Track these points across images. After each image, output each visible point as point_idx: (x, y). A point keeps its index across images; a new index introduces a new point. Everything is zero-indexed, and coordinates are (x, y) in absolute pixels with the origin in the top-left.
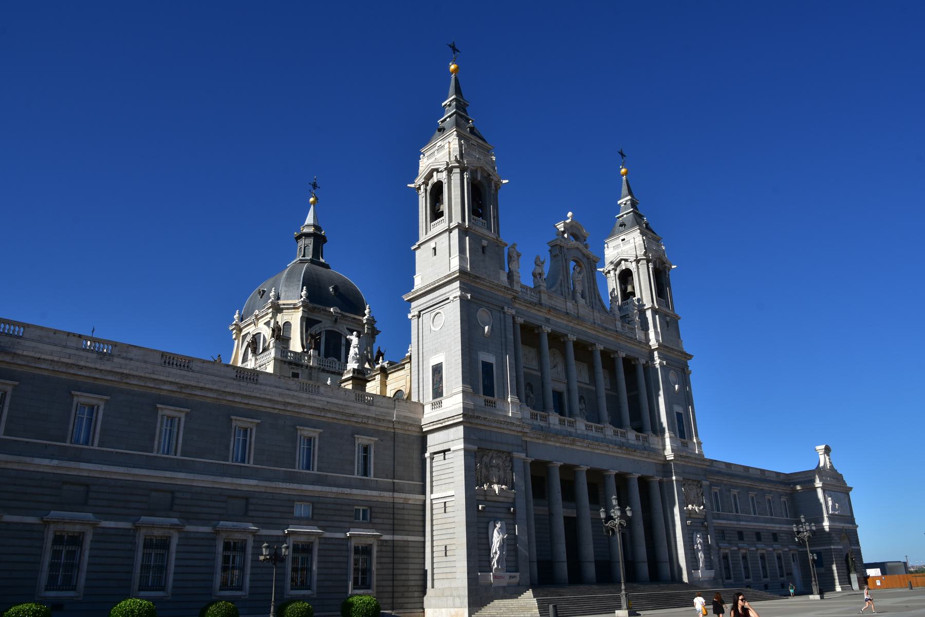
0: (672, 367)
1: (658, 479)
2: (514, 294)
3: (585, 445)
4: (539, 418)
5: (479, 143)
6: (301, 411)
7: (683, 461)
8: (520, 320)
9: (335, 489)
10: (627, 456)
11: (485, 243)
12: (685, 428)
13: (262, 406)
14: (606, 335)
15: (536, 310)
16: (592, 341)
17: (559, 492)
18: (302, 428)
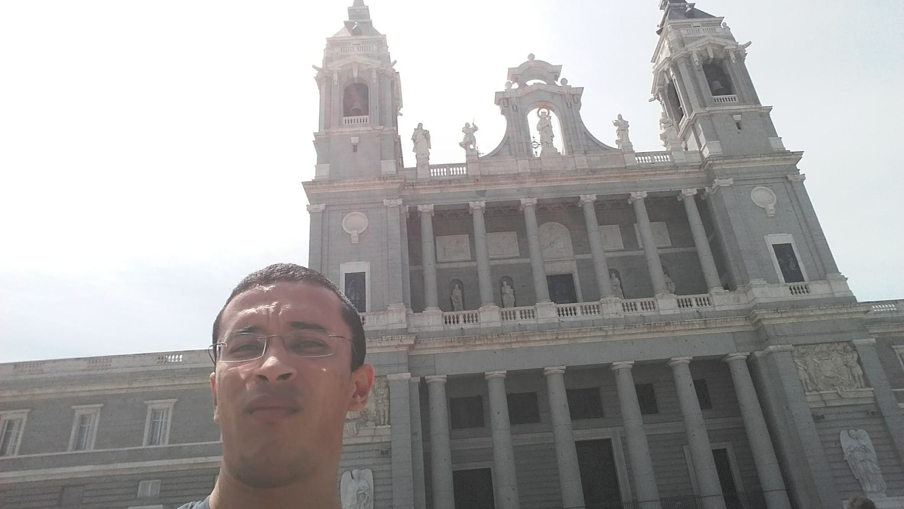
0: (756, 182)
1: (742, 356)
2: (397, 181)
3: (550, 337)
4: (461, 319)
5: (364, 39)
6: (150, 385)
7: (789, 317)
8: (426, 208)
9: (184, 461)
10: (657, 335)
11: (355, 140)
12: (801, 265)
13: (108, 390)
14: (601, 178)
15: (456, 187)
16: (574, 195)
17: (498, 413)
18: (150, 402)
